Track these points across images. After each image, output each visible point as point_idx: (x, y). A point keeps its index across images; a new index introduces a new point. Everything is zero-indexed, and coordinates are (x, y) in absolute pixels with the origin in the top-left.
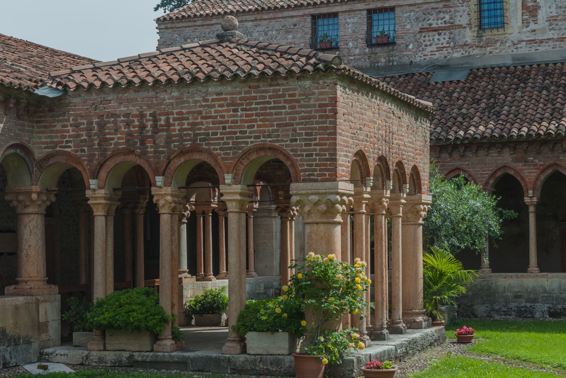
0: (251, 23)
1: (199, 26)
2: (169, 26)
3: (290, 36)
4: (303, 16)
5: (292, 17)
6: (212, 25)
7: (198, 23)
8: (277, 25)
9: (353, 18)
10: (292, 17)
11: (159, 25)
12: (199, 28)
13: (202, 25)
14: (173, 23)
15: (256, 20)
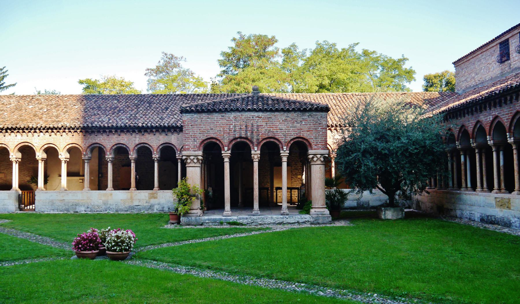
0: (480, 56)
1: (466, 62)
2: (457, 65)
3: (493, 58)
4: (497, 45)
5: (493, 47)
6: (469, 60)
7: (465, 60)
8: (488, 53)
9: (514, 39)
10: (493, 47)
11: (455, 65)
12: (465, 63)
13: (467, 61)
14: (458, 63)
15: (481, 53)
